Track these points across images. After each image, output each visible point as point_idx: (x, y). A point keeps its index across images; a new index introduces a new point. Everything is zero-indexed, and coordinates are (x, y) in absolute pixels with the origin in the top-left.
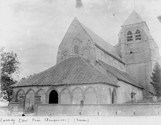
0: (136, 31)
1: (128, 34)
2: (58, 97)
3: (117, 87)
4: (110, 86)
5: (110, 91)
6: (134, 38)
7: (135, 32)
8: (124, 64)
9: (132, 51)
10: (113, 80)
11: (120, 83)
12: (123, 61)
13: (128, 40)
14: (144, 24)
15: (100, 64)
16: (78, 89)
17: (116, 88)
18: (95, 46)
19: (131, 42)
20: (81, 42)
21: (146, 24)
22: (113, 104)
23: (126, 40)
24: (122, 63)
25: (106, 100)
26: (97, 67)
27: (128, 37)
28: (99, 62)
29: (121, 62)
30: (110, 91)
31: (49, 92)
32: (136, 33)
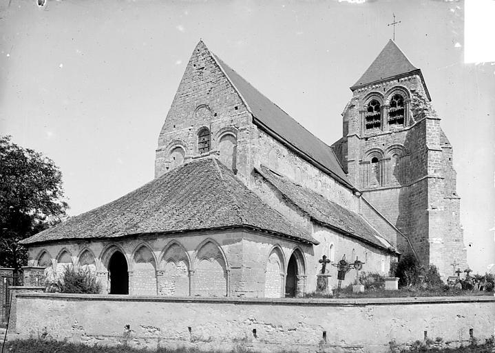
0: (392, 99)
1: (370, 110)
2: (128, 270)
3: (309, 244)
4: (278, 241)
5: (281, 255)
6: (386, 117)
7: (387, 102)
8: (354, 191)
9: (376, 157)
10: (298, 224)
11: (318, 235)
12: (350, 181)
13: (369, 127)
14: (418, 77)
15: (264, 179)
16: (175, 247)
17: (303, 248)
18: (252, 125)
19: (377, 131)
20: (216, 115)
21: (422, 77)
22: (293, 300)
23: (364, 126)
24: (347, 187)
25: (261, 281)
26: (252, 185)
27: (369, 118)
28: (262, 173)
29: (345, 185)
30: (281, 255)
31: (107, 258)
32: (393, 104)
